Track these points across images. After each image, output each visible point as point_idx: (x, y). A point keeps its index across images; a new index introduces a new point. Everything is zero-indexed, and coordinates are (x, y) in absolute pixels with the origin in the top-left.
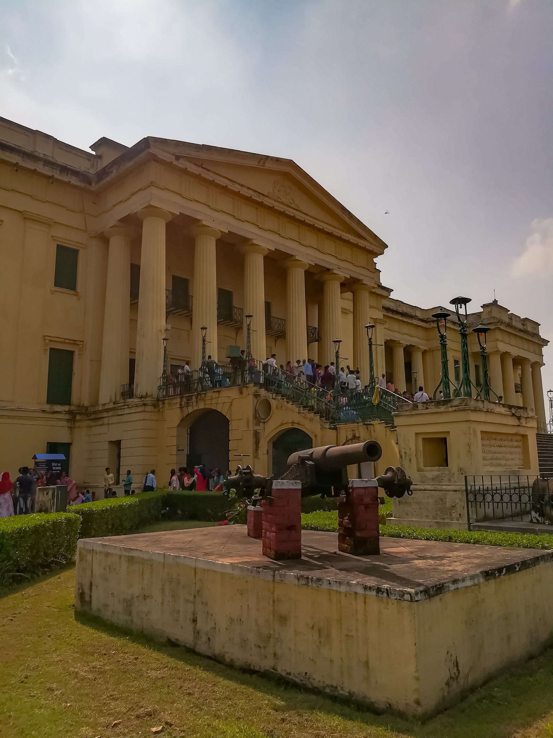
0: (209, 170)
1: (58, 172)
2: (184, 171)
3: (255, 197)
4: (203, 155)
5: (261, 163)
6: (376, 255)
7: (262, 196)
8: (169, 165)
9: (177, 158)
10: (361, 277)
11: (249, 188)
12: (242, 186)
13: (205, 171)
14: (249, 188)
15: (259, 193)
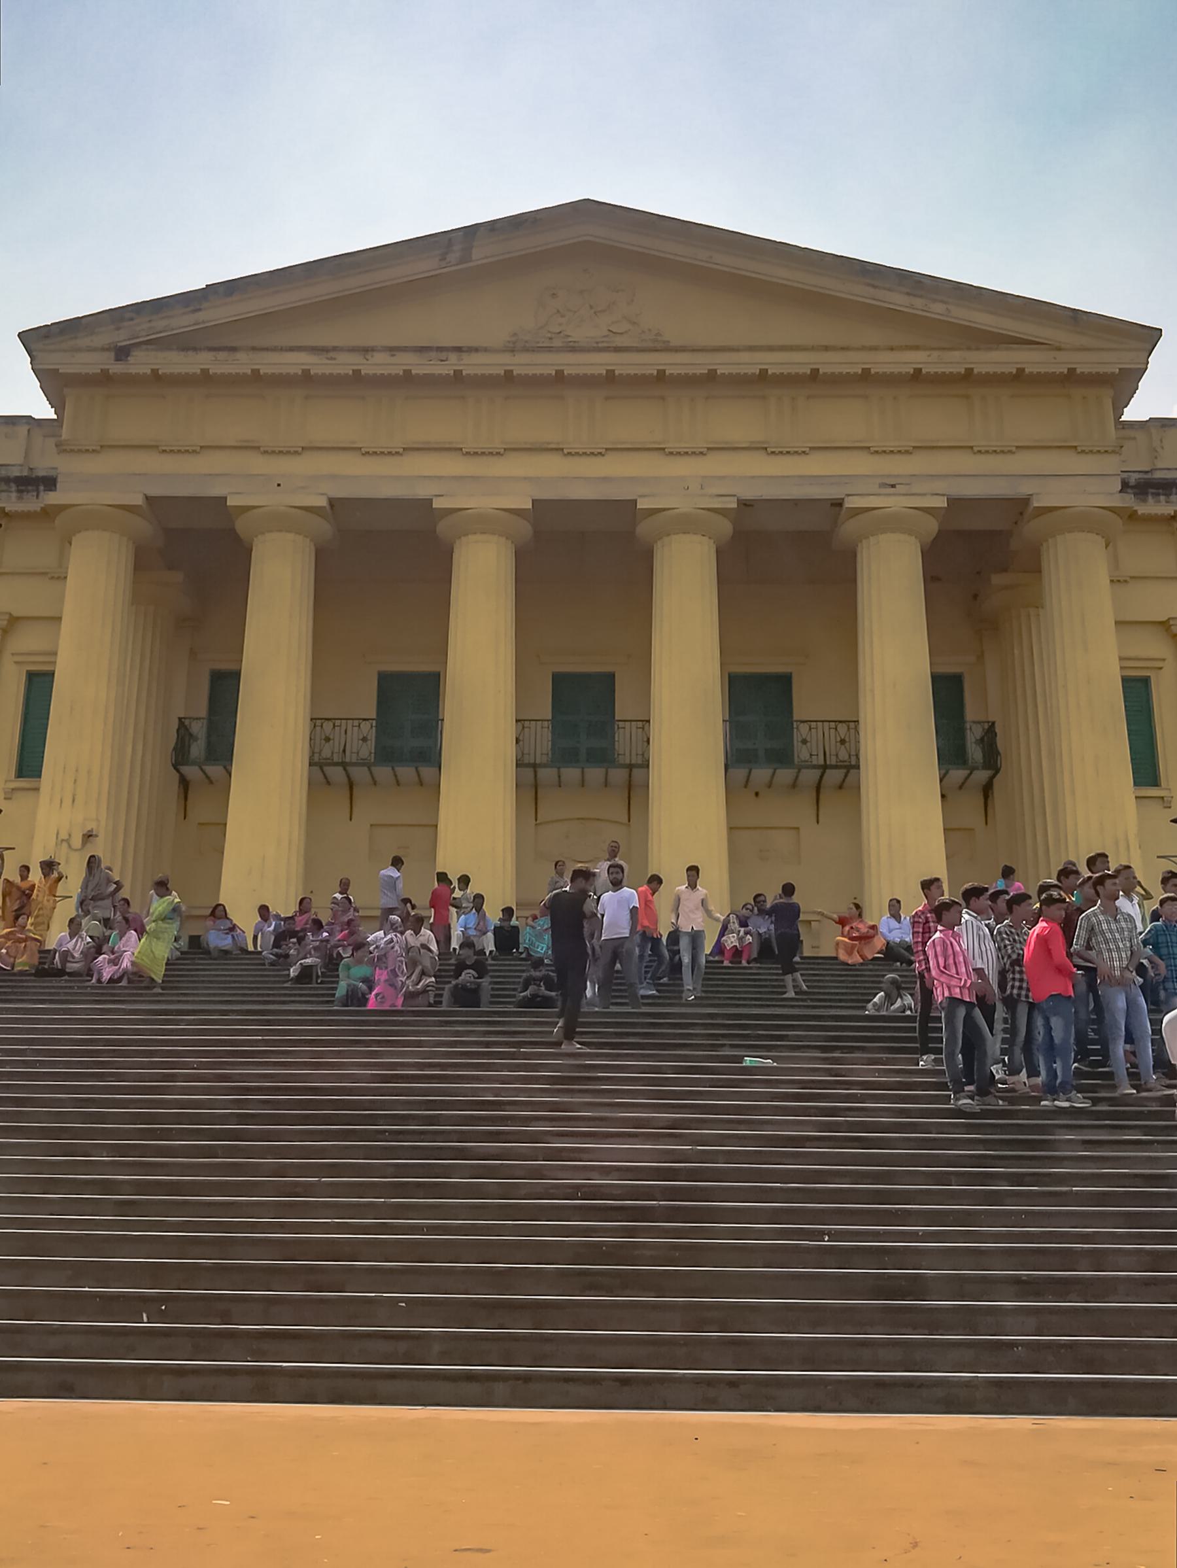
0: (233, 349)
1: (14, 495)
2: (156, 377)
3: (421, 366)
4: (214, 314)
5: (453, 257)
6: (1125, 382)
7: (453, 357)
8: (105, 379)
9: (122, 353)
10: (1024, 489)
11: (392, 350)
12: (366, 350)
13: (222, 355)
14: (392, 350)
15: (440, 349)
